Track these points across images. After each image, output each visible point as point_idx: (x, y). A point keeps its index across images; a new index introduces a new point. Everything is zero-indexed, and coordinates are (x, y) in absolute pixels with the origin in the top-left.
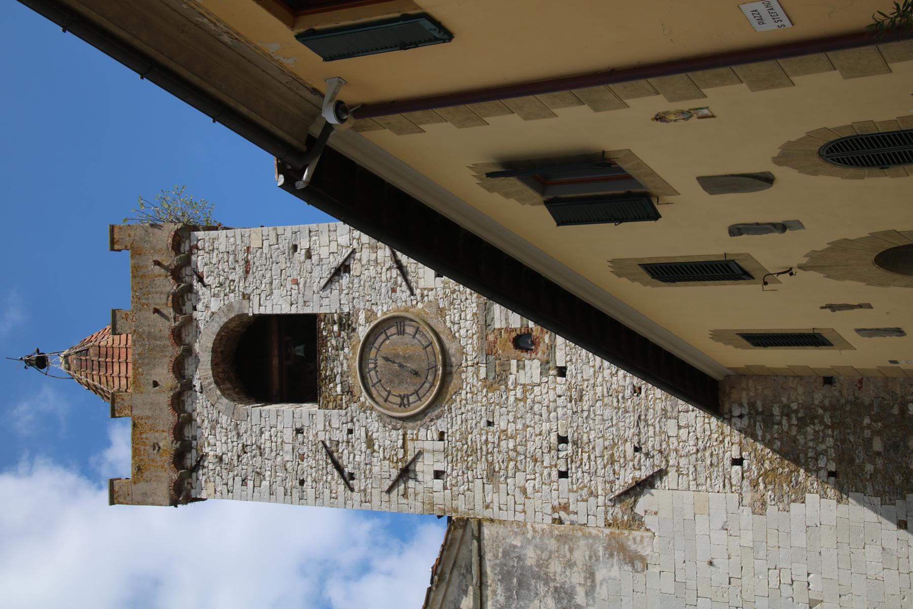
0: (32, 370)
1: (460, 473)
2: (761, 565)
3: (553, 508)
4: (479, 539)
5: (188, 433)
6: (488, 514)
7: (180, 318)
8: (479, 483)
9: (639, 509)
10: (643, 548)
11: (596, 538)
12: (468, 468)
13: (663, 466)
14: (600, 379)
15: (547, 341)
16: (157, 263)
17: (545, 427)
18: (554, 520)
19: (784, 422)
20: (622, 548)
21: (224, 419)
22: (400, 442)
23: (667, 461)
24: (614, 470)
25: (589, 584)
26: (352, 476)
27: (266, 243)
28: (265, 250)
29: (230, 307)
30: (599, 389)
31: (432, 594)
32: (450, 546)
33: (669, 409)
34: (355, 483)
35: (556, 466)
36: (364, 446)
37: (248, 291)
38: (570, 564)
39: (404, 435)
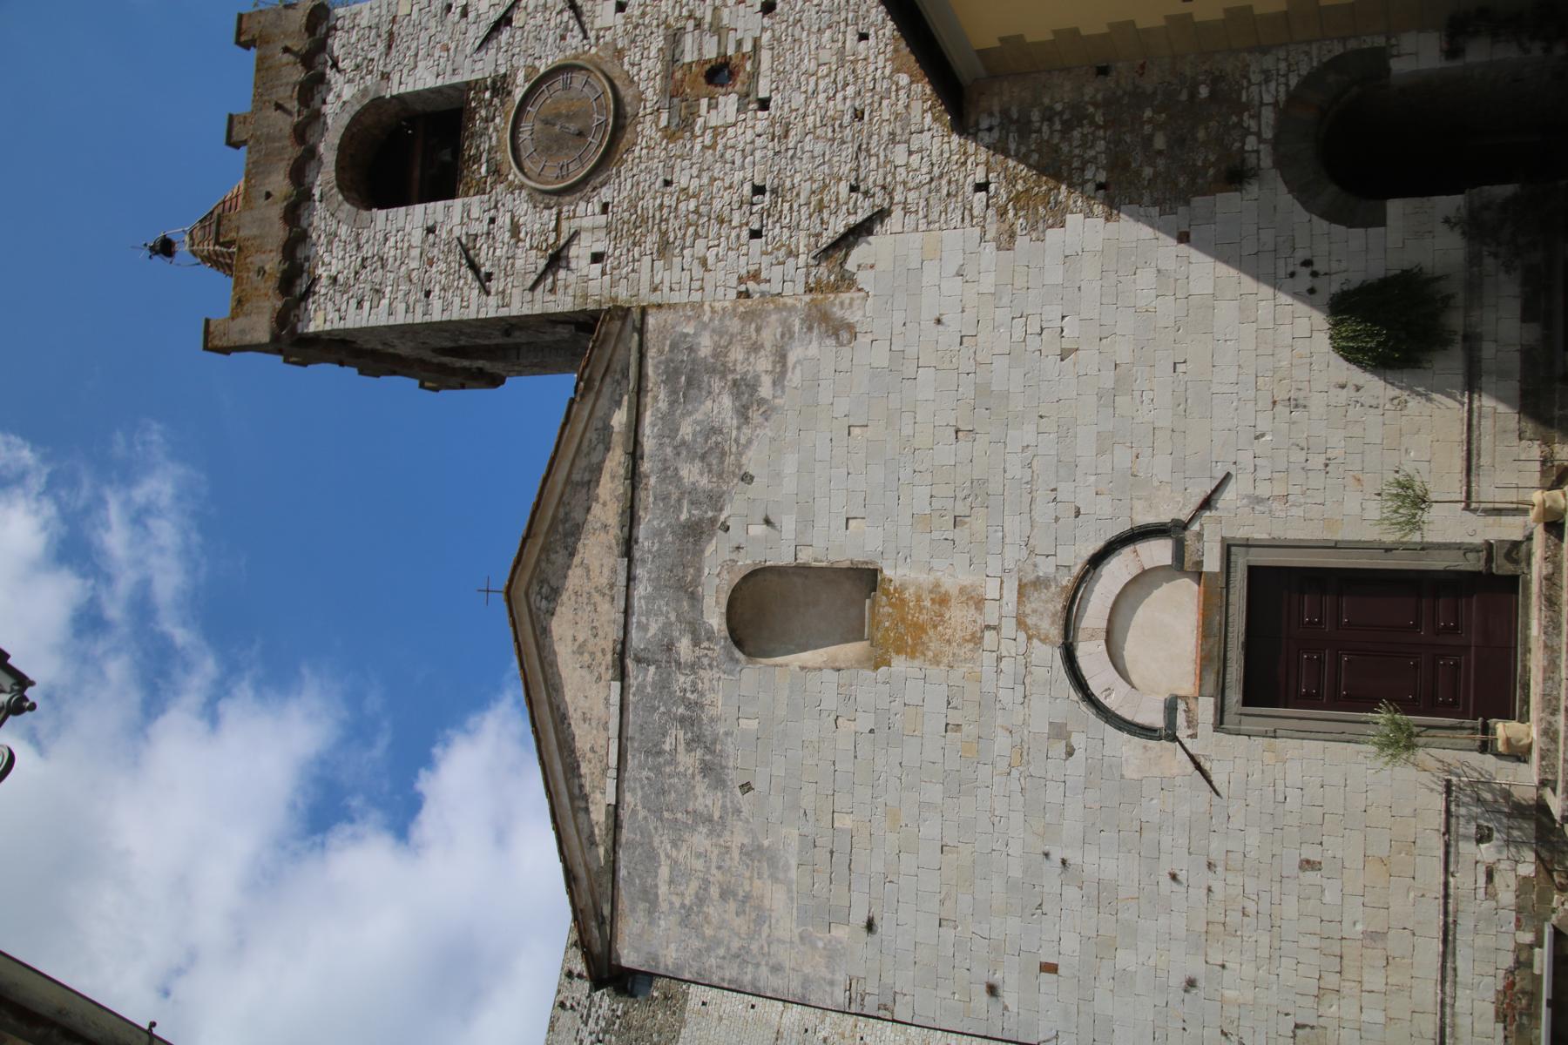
0: (159, 260)
2: (1003, 315)
3: (741, 280)
4: (641, 331)
5: (300, 254)
6: (656, 298)
7: (305, 112)
8: (647, 260)
9: (850, 265)
11: (794, 306)
12: (634, 244)
13: (886, 205)
14: (813, 106)
15: (748, 67)
16: (286, 50)
17: (738, 176)
18: (740, 294)
19: (1045, 128)
21: (343, 231)
23: (892, 198)
26: (489, 276)
27: (416, 8)
28: (414, 16)
29: (365, 91)
30: (810, 120)
31: (575, 407)
32: (604, 342)
33: (899, 131)
34: (493, 286)
36: (508, 235)
37: (388, 69)
38: (756, 348)
39: (559, 214)
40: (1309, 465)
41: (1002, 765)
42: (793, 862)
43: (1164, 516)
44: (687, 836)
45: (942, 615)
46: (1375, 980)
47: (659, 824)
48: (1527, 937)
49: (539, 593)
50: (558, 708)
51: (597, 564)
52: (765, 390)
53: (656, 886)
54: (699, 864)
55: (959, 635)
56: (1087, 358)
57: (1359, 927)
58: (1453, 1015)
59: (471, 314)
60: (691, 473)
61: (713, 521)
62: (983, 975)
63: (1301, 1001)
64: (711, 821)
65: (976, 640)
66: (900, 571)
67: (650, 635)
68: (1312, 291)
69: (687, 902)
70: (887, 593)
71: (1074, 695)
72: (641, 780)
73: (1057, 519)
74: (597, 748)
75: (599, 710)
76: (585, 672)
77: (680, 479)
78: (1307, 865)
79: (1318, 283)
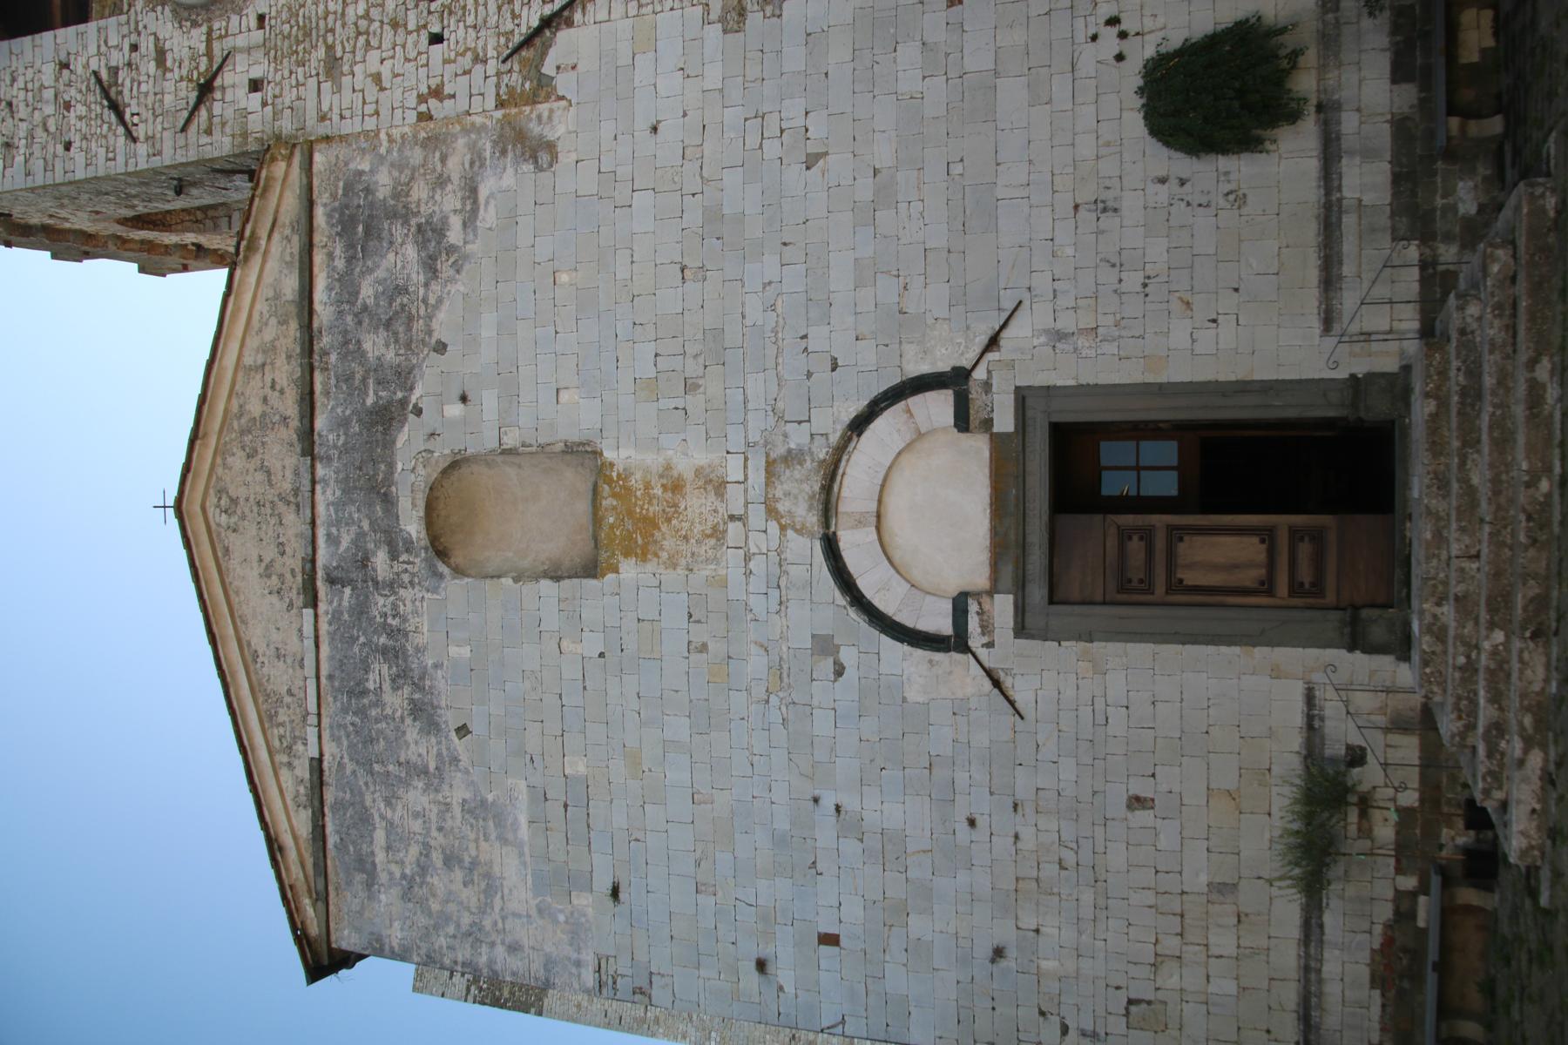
1: (286, 73)
2: (733, 115)
3: (422, 99)
6: (324, 129)
8: (313, 82)
9: (548, 68)
10: (553, 127)
11: (484, 126)
20: (521, 136)
22: (202, 48)
24: (513, 11)
25: (468, 208)
32: (265, 190)
35: (425, 26)
36: (153, 64)
38: (441, 182)
40: (1124, 287)
41: (759, 691)
42: (523, 820)
43: (942, 362)
44: (401, 792)
45: (676, 506)
46: (1224, 942)
47: (369, 779)
48: (1409, 883)
49: (218, 506)
50: (249, 644)
51: (278, 465)
52: (454, 235)
53: (372, 853)
54: (417, 826)
55: (698, 528)
56: (838, 162)
57: (1203, 879)
58: (1320, 981)
59: (119, 167)
60: (374, 345)
61: (404, 403)
62: (751, 951)
63: (1134, 971)
64: (426, 773)
65: (718, 534)
66: (624, 453)
67: (342, 549)
68: (1120, 57)
69: (408, 871)
70: (609, 481)
71: (841, 600)
72: (345, 727)
73: (809, 375)
74: (295, 691)
75: (293, 645)
76: (274, 599)
77: (363, 354)
78: (1137, 802)
79: (1126, 46)
